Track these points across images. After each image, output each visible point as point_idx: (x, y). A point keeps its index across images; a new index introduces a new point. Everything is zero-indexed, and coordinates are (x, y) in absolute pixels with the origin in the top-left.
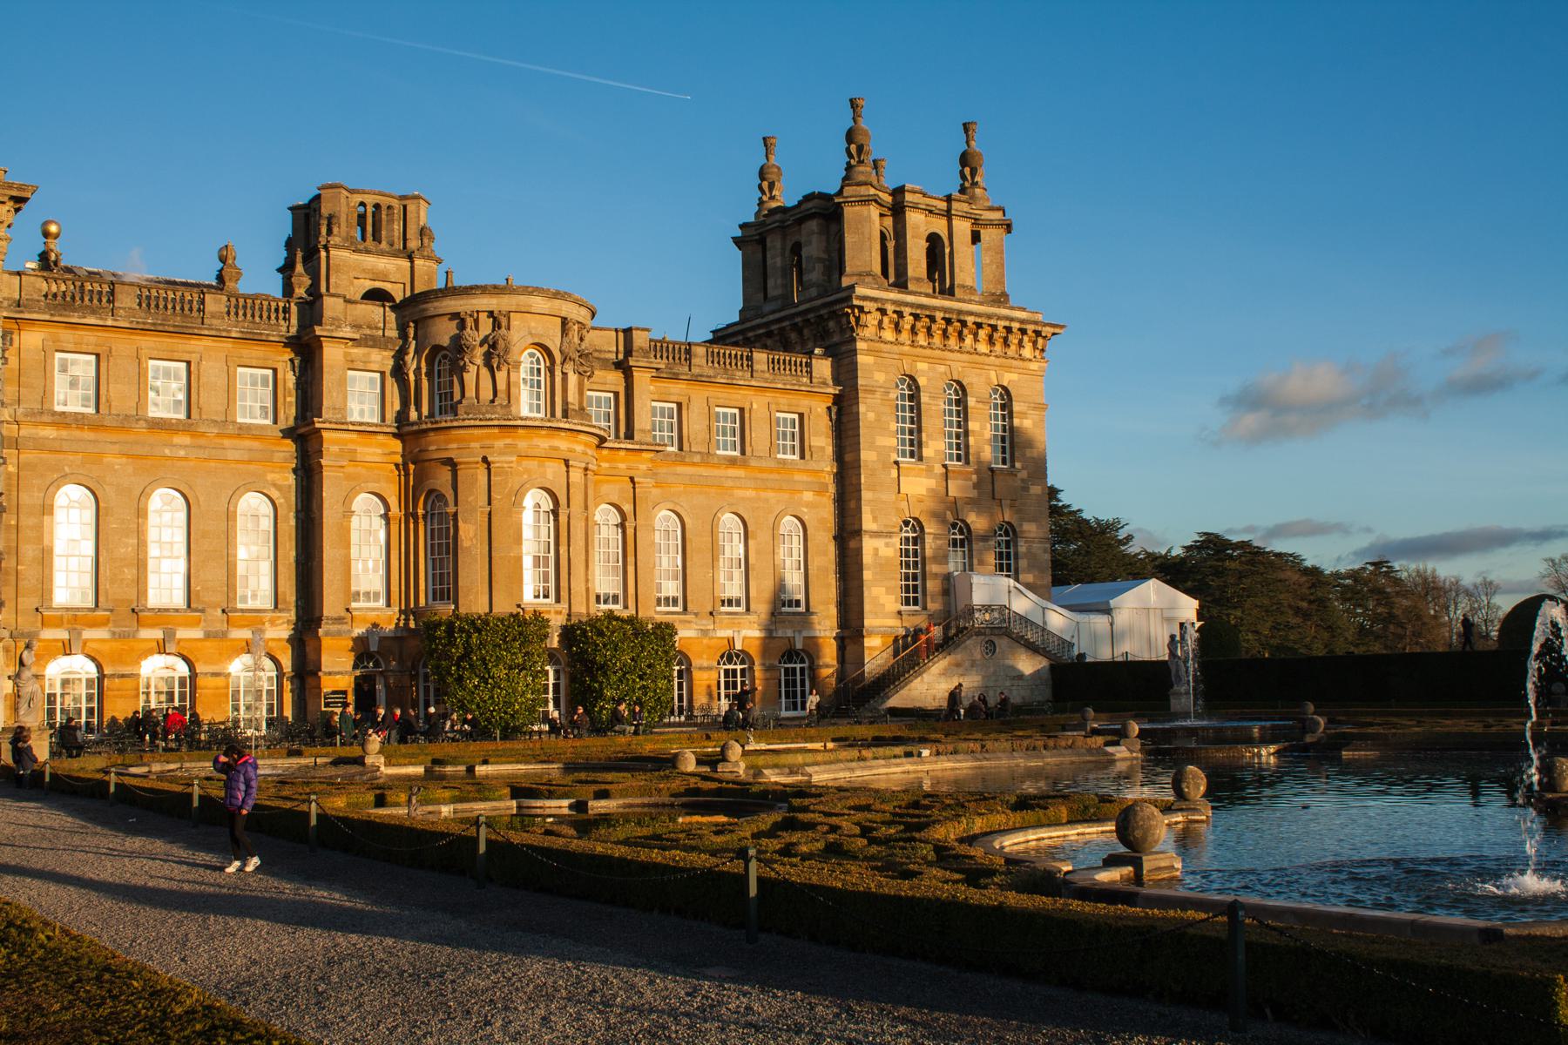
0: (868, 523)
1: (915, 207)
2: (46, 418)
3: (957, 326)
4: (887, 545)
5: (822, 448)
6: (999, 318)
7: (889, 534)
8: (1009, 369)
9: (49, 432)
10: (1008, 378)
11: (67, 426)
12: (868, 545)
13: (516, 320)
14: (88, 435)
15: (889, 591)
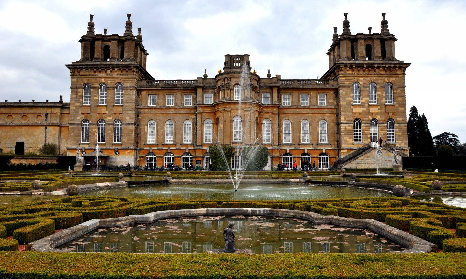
0: (343, 120)
1: (360, 38)
2: (146, 108)
3: (371, 67)
4: (349, 126)
5: (333, 103)
6: (386, 64)
7: (350, 123)
8: (392, 77)
9: (147, 110)
10: (391, 80)
11: (150, 109)
12: (343, 127)
13: (232, 79)
14: (154, 110)
15: (350, 138)
